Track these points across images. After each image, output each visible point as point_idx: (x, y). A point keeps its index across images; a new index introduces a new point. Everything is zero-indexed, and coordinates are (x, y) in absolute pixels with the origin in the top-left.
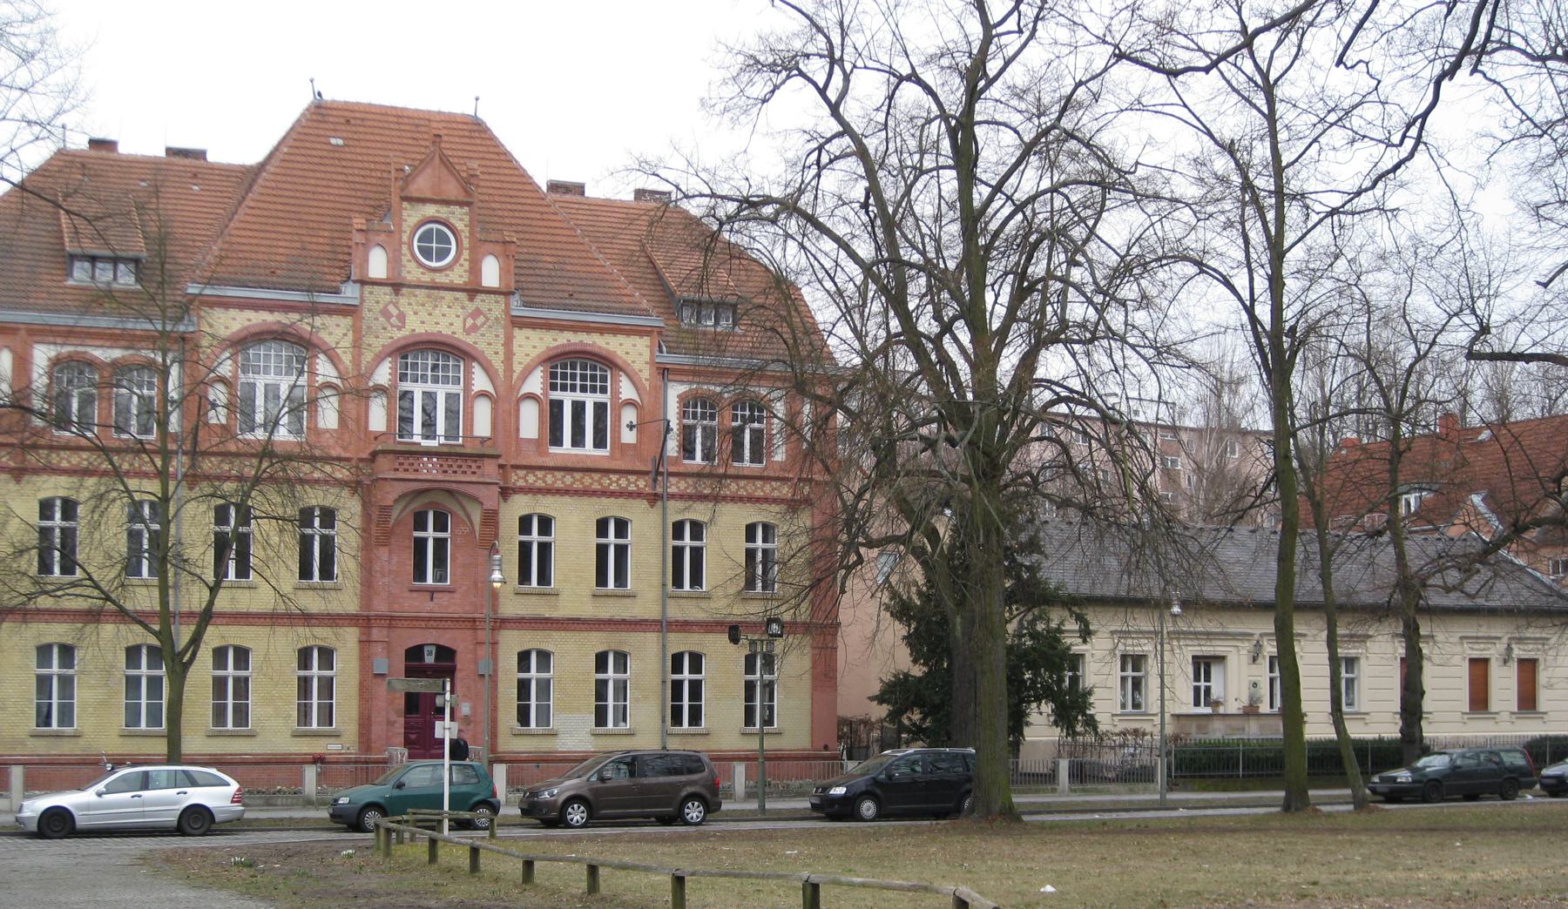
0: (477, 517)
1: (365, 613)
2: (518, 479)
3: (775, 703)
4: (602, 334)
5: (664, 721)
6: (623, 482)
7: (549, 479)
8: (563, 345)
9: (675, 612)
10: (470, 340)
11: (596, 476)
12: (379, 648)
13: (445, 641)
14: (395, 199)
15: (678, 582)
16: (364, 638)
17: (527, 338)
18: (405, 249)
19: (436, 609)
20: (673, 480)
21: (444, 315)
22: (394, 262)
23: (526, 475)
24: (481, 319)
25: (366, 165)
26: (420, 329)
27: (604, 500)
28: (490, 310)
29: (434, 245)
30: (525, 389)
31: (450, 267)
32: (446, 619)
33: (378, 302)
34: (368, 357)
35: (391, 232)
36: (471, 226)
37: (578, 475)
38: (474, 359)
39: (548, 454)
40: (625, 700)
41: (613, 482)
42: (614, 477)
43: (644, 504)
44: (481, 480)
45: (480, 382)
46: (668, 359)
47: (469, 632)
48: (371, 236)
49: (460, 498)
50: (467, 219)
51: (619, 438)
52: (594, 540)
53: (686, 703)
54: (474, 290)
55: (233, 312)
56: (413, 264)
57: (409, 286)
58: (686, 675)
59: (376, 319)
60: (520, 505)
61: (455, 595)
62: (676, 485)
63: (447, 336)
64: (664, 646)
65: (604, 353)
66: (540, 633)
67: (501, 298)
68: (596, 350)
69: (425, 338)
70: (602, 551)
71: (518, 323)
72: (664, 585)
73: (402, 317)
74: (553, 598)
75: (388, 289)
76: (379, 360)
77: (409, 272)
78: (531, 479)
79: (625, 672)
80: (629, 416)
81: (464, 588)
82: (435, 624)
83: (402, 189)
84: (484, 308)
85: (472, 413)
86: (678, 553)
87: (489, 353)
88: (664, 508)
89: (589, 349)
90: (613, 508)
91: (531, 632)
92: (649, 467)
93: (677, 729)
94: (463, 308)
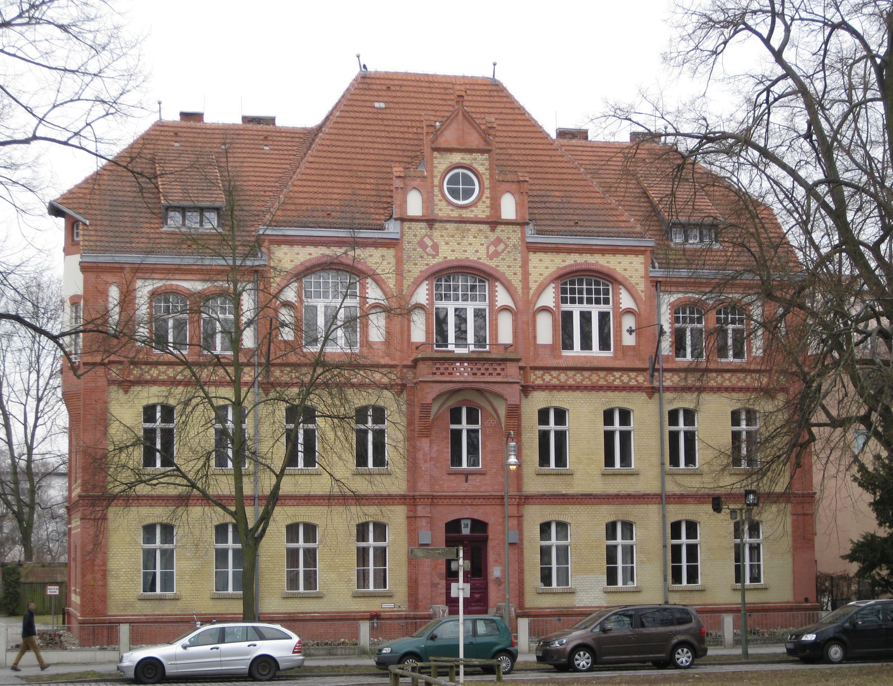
0: (502, 411)
2: (536, 378)
4: (603, 254)
5: (665, 580)
6: (625, 378)
7: (563, 377)
8: (571, 266)
9: (672, 488)
10: (492, 264)
15: (674, 461)
17: (541, 260)
18: (436, 190)
20: (668, 375)
21: (470, 244)
22: (428, 202)
23: (543, 375)
24: (501, 247)
26: (451, 257)
27: (610, 394)
28: (509, 238)
31: (474, 204)
33: (415, 236)
34: (408, 282)
35: (424, 177)
36: (491, 169)
37: (587, 374)
38: (497, 280)
39: (561, 357)
40: (632, 563)
41: (617, 379)
42: (617, 374)
43: (644, 396)
44: (505, 380)
45: (503, 298)
46: (658, 273)
47: (498, 508)
49: (488, 395)
50: (487, 163)
51: (621, 341)
52: (602, 428)
53: (684, 564)
54: (495, 222)
55: (297, 249)
56: (444, 203)
57: (441, 221)
58: (684, 540)
59: (415, 250)
60: (539, 400)
61: (487, 477)
62: (670, 380)
63: (473, 261)
64: (664, 516)
65: (605, 270)
66: (559, 507)
67: (518, 228)
68: (599, 268)
69: (456, 264)
71: (533, 248)
72: (663, 464)
73: (435, 247)
74: (569, 477)
75: (423, 225)
76: (417, 284)
77: (441, 210)
78: (547, 377)
79: (632, 538)
80: (629, 322)
81: (494, 470)
84: (504, 236)
85: (497, 325)
87: (509, 274)
88: (661, 399)
90: (618, 400)
91: (552, 507)
92: (647, 365)
93: (677, 586)
94: (486, 237)
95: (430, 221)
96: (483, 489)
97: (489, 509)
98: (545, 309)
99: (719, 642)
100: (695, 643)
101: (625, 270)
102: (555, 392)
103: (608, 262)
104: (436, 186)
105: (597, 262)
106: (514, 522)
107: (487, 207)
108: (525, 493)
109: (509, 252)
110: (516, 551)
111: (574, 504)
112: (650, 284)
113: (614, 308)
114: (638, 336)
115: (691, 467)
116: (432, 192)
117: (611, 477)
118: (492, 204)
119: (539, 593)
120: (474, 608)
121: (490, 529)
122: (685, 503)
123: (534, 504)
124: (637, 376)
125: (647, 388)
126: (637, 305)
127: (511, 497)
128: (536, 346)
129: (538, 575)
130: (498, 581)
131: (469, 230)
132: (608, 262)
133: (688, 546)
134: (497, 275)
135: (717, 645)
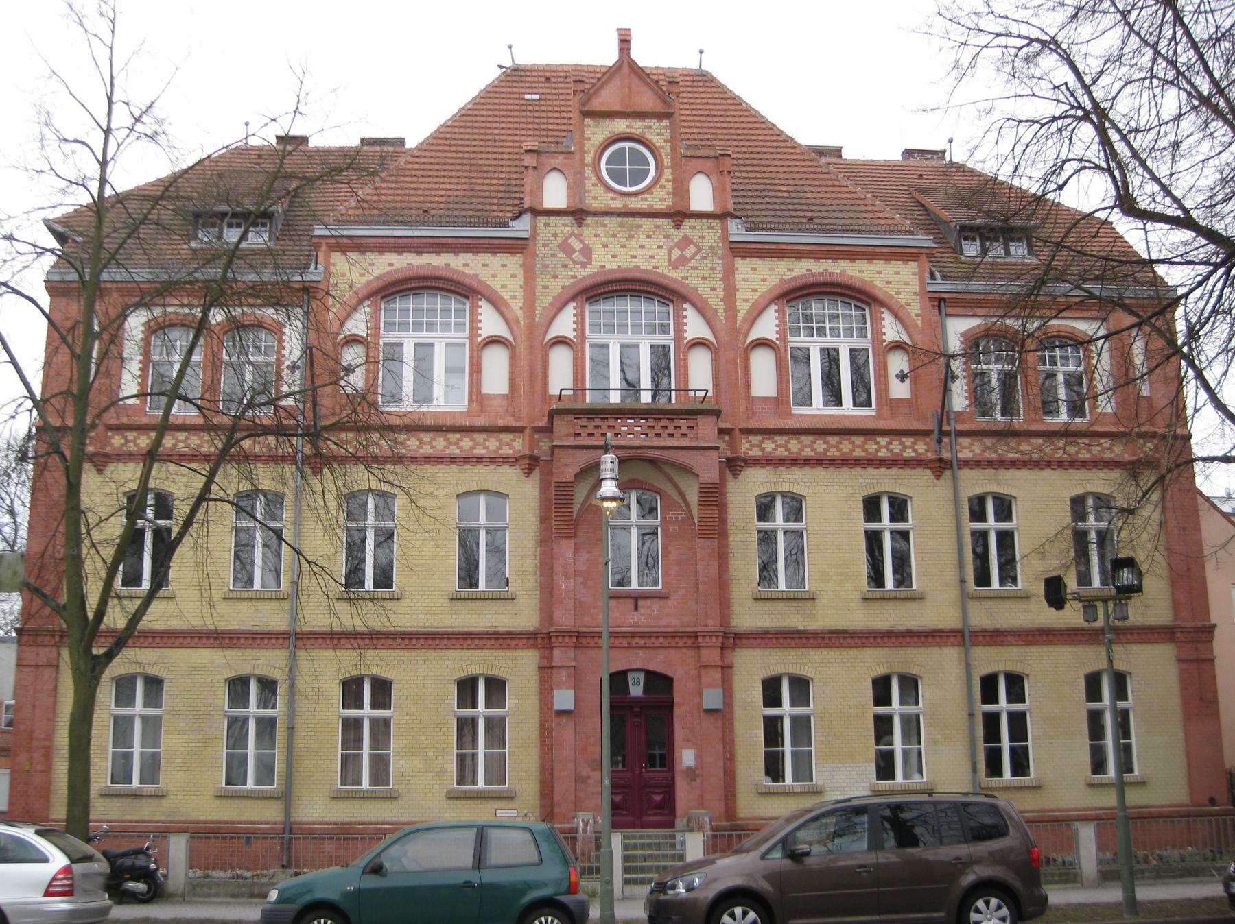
0: (693, 497)
1: (545, 630)
2: (750, 447)
3: (1133, 740)
4: (853, 260)
5: (974, 770)
6: (896, 447)
7: (794, 445)
8: (802, 276)
9: (981, 617)
10: (677, 275)
11: (858, 440)
12: (563, 675)
13: (657, 663)
14: (575, 115)
15: (983, 578)
16: (545, 663)
17: (754, 269)
18: (588, 172)
19: (643, 622)
20: (965, 441)
21: (642, 247)
22: (576, 187)
23: (762, 442)
24: (691, 249)
25: (562, 115)
26: (612, 265)
27: (872, 472)
28: (702, 237)
29: (628, 167)
30: (755, 334)
31: (648, 190)
32: (657, 635)
33: (555, 235)
34: (544, 300)
35: (572, 153)
36: (673, 140)
37: (833, 440)
38: (685, 299)
39: (792, 416)
40: (919, 743)
41: (882, 447)
42: (883, 441)
43: (927, 475)
45: (695, 327)
46: (941, 286)
47: (690, 653)
48: (544, 158)
49: (668, 470)
50: (667, 133)
51: (887, 391)
52: (860, 525)
53: (1006, 744)
54: (680, 215)
55: (371, 256)
56: (600, 189)
57: (595, 214)
58: (1003, 705)
59: (554, 255)
60: (755, 482)
61: (671, 602)
62: (968, 449)
63: (647, 271)
64: (968, 665)
65: (857, 284)
66: (792, 652)
67: (716, 223)
68: (846, 280)
69: (619, 276)
70: (874, 540)
71: (739, 250)
72: (963, 581)
73: (587, 251)
74: (809, 604)
75: (568, 220)
76: (558, 307)
77: (595, 198)
78: (769, 446)
79: (917, 704)
80: (898, 363)
81: (681, 592)
82: (642, 642)
83: (584, 104)
84: (694, 235)
85: (686, 367)
86: (980, 537)
87: (703, 290)
88: (955, 479)
89: (835, 279)
90: (885, 482)
91: (780, 652)
92: (932, 425)
93: (995, 781)
94: (667, 237)
95: (578, 214)
96: (663, 623)
97: (674, 655)
98: (763, 343)
99: (1070, 876)
100: (1017, 884)
101: (889, 283)
102: (782, 469)
103: (861, 272)
104: (588, 165)
105: (844, 271)
106: (717, 675)
107: (668, 193)
108: (733, 630)
109: (703, 258)
110: (719, 723)
111: (818, 646)
112: (929, 304)
113: (873, 343)
114: (915, 383)
115: (1009, 587)
116: (582, 172)
117: (878, 604)
118: (674, 189)
119: (761, 794)
120: (652, 819)
121: (677, 686)
122: (1001, 644)
123: (751, 647)
124: (914, 444)
125: (932, 461)
126: (910, 336)
127: (711, 634)
128: (751, 400)
129: (761, 763)
130: (691, 773)
131: (640, 226)
132: (861, 272)
133: (1011, 715)
134: (684, 291)
135: (1066, 881)
